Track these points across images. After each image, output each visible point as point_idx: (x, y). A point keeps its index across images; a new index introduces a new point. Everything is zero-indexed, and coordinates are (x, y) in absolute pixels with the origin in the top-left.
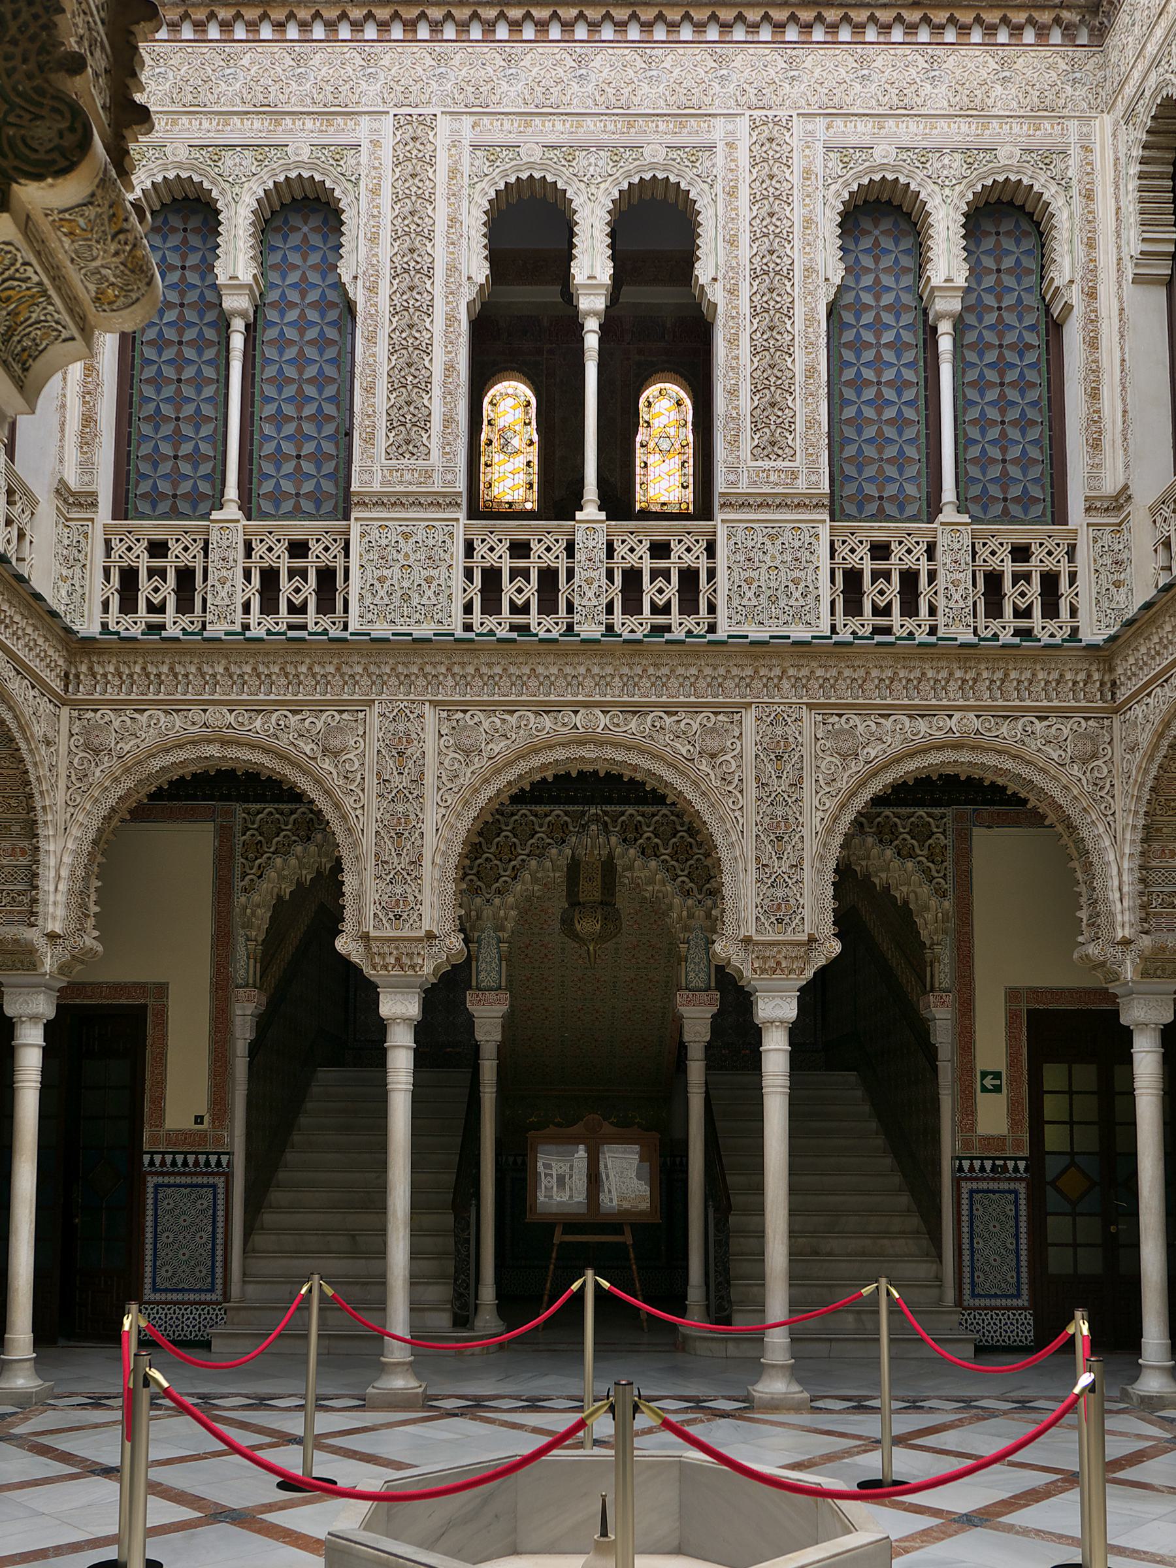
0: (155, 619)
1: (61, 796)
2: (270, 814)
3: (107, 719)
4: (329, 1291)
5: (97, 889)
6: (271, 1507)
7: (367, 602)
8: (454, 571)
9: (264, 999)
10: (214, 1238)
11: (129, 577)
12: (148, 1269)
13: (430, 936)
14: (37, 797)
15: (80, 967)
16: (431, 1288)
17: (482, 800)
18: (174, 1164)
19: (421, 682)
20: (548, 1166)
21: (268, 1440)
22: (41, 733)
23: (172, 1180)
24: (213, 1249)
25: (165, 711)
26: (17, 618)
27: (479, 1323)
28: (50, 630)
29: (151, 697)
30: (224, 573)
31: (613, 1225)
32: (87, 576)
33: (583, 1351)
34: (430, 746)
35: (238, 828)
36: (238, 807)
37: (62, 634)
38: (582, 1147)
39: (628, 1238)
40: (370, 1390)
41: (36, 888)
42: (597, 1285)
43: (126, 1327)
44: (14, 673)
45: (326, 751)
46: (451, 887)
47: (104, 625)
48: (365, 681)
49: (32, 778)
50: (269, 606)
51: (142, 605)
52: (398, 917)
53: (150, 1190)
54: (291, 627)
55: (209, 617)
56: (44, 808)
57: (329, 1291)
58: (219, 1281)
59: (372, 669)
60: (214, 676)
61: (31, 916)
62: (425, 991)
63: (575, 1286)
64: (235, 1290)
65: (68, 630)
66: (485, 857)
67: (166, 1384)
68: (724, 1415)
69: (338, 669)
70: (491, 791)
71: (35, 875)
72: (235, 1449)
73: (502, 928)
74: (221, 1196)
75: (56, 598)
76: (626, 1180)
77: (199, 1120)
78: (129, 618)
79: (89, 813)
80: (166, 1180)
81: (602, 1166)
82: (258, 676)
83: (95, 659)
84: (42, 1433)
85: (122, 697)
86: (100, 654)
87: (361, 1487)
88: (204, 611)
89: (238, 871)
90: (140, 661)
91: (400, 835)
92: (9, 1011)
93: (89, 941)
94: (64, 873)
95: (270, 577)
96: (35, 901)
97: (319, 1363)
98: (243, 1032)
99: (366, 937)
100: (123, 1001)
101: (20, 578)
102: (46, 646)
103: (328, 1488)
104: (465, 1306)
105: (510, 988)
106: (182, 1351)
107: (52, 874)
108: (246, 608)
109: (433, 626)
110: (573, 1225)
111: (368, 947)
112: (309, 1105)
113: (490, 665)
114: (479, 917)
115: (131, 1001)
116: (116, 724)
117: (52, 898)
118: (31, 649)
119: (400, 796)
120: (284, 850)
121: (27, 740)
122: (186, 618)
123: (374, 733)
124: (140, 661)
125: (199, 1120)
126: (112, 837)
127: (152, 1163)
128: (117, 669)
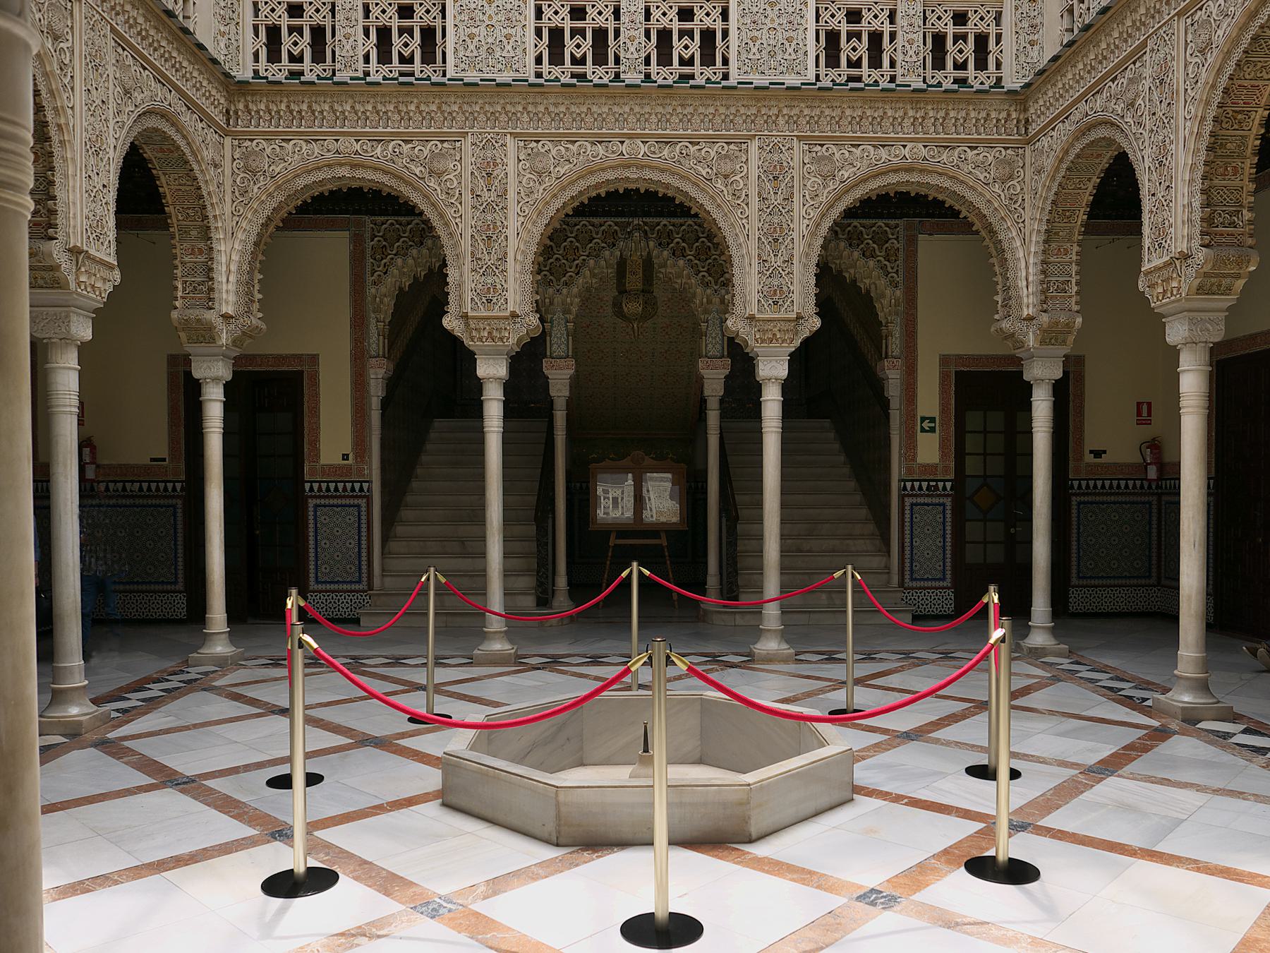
0: (296, 67)
1: (228, 208)
2: (392, 224)
3: (261, 147)
4: (443, 580)
5: (260, 281)
6: (403, 735)
7: (461, 54)
8: (527, 30)
9: (391, 367)
10: (360, 544)
11: (274, 34)
12: (312, 567)
13: (514, 315)
14: (209, 208)
15: (248, 341)
16: (520, 579)
17: (551, 211)
18: (328, 489)
19: (503, 118)
20: (606, 492)
21: (402, 688)
22: (210, 157)
23: (327, 502)
24: (359, 552)
25: (306, 141)
26: (185, 64)
27: (555, 603)
28: (213, 74)
29: (294, 129)
30: (348, 30)
31: (654, 531)
32: (240, 32)
33: (630, 622)
34: (511, 168)
35: (368, 235)
36: (367, 219)
37: (222, 78)
38: (630, 475)
39: (663, 541)
40: (476, 652)
41: (212, 279)
42: (640, 573)
43: (289, 606)
44: (185, 108)
45: (431, 172)
46: (529, 278)
47: (256, 72)
48: (460, 118)
49: (205, 193)
50: (384, 58)
51: (285, 56)
52: (489, 301)
53: (311, 509)
54: (402, 74)
55: (338, 66)
56: (215, 217)
57: (443, 580)
58: (365, 575)
59: (465, 107)
60: (343, 112)
61: (209, 301)
62: (511, 358)
63: (624, 574)
64: (377, 582)
65: (227, 75)
66: (556, 253)
67: (315, 646)
68: (733, 666)
69: (439, 108)
70: (558, 204)
71: (211, 270)
72: (373, 695)
73: (569, 312)
74: (364, 513)
75: (216, 49)
76: (662, 501)
77: (345, 457)
78: (275, 66)
79: (250, 221)
80: (323, 501)
81: (644, 490)
82: (378, 113)
83: (249, 98)
84: (236, 685)
85: (272, 129)
86: (253, 95)
87: (468, 720)
88: (334, 61)
89: (368, 269)
90: (285, 100)
91: (489, 238)
92: (196, 374)
93: (255, 320)
94: (233, 268)
95: (384, 34)
96: (211, 290)
97: (436, 633)
98: (376, 391)
99: (465, 317)
100: (285, 368)
101: (186, 31)
102: (210, 87)
103: (445, 721)
104: (545, 592)
105: (575, 356)
106: (338, 627)
107: (224, 269)
108: (367, 59)
109: (512, 74)
110: (623, 531)
111: (467, 325)
112: (428, 447)
113: (556, 105)
114: (551, 303)
115: (291, 369)
116: (268, 151)
117: (224, 287)
118: (155, 50)
119: (489, 207)
120: (403, 253)
121: (198, 162)
122: (320, 67)
123: (468, 159)
124: (285, 100)
125: (345, 457)
126: (269, 240)
127: (311, 489)
128: (267, 107)
